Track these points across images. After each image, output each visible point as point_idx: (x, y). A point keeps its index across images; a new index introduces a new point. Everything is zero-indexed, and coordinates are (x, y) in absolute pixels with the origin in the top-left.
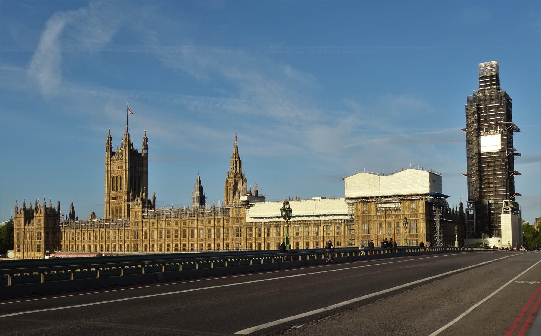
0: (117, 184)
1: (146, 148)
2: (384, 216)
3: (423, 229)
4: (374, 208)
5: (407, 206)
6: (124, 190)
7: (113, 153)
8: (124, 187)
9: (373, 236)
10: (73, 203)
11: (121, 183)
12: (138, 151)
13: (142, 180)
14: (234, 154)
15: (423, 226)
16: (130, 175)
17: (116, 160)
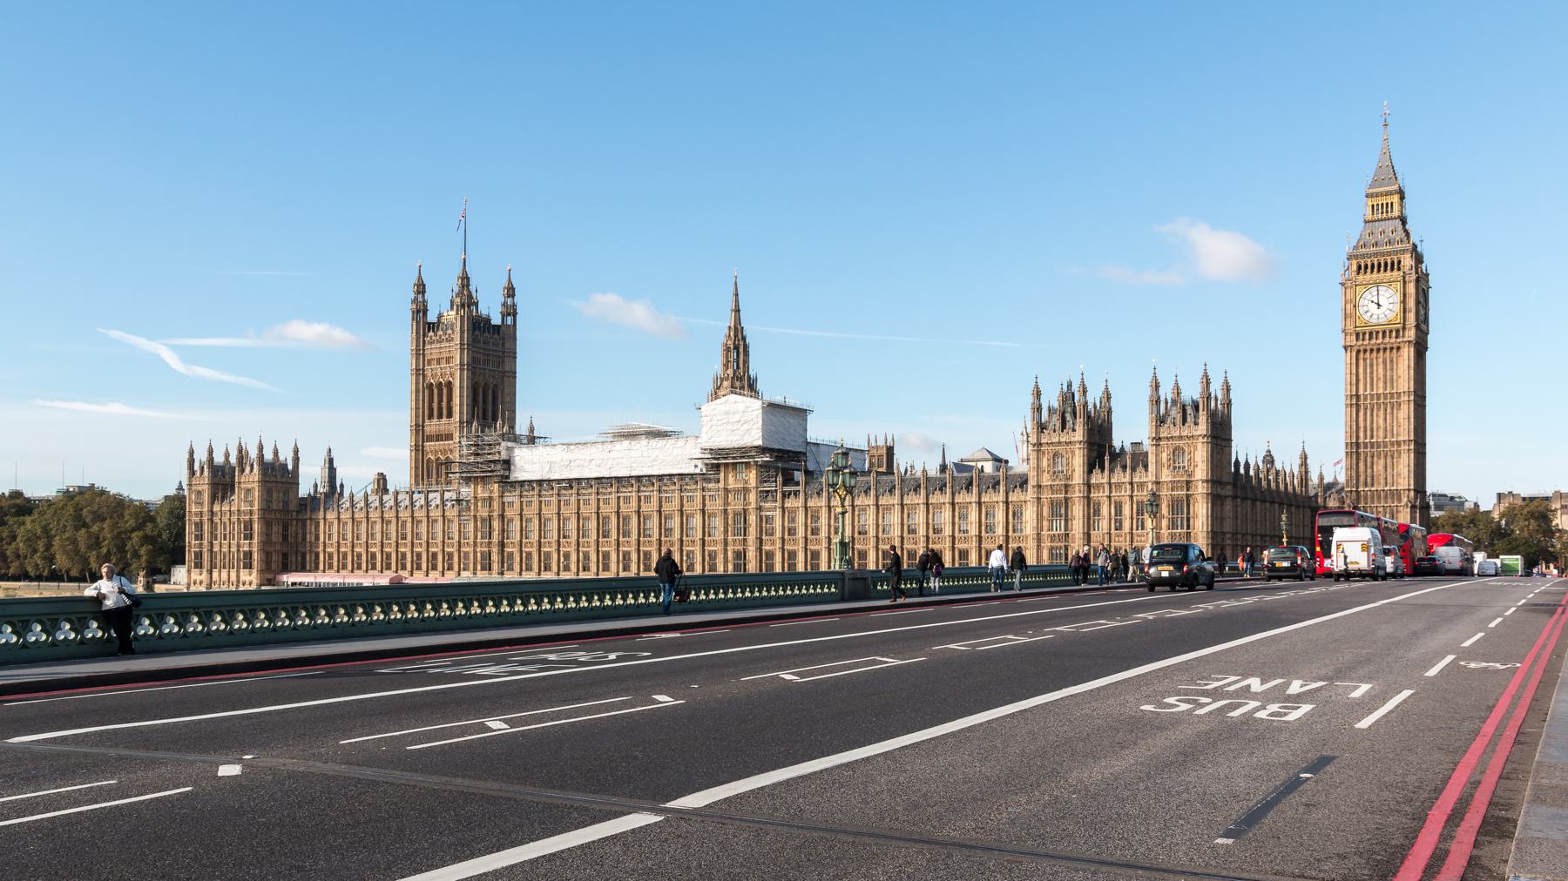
0: (440, 401)
1: (510, 311)
2: (1107, 487)
3: (1205, 518)
4: (1080, 466)
6: (457, 417)
7: (429, 324)
8: (456, 409)
9: (1077, 536)
10: (330, 450)
11: (450, 399)
12: (490, 320)
13: (503, 391)
15: (1205, 511)
16: (472, 380)
17: (438, 341)
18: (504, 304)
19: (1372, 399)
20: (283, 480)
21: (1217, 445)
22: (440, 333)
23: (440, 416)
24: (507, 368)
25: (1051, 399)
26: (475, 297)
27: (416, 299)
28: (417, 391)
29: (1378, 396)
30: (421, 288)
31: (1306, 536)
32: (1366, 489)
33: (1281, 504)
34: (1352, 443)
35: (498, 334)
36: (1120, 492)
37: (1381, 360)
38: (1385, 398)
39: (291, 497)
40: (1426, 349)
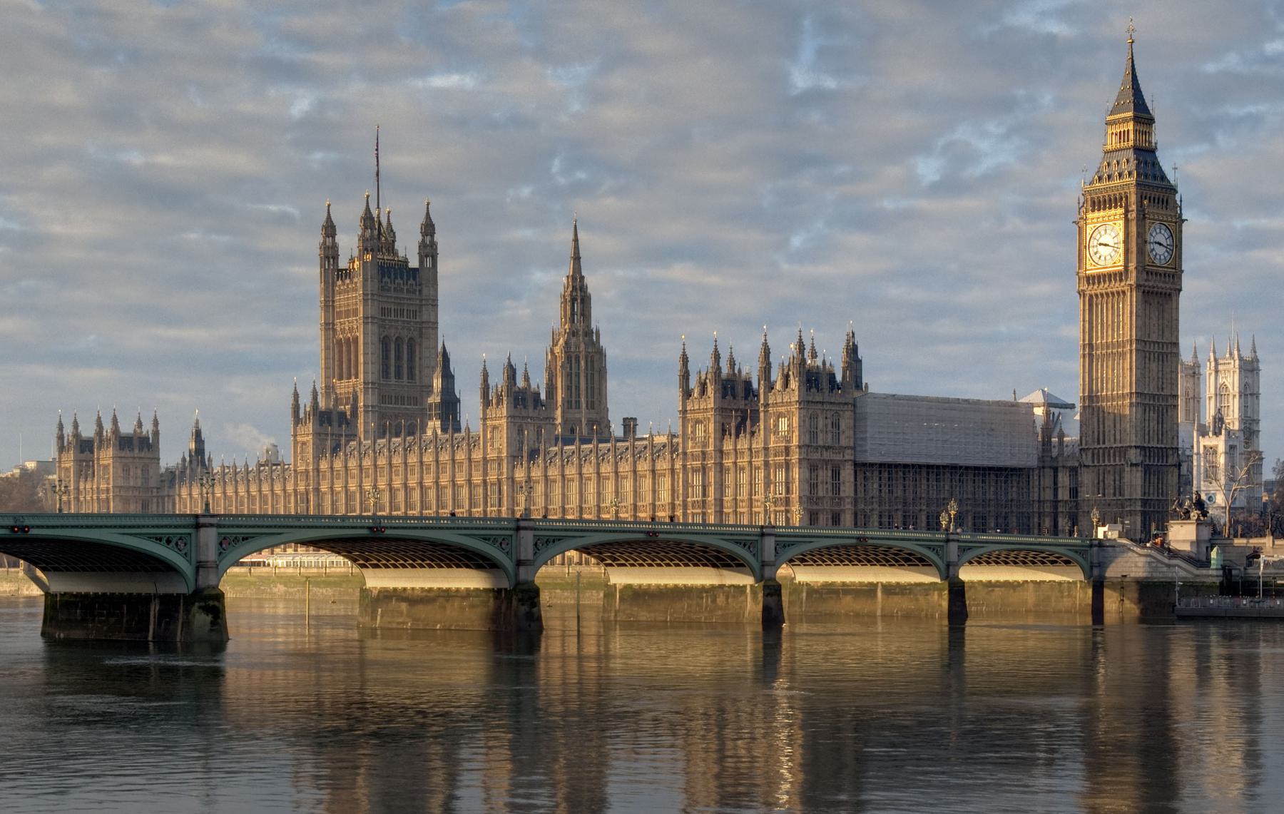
0: (349, 360)
1: (429, 250)
5: (772, 427)
6: (361, 376)
7: (342, 270)
12: (406, 262)
13: (420, 345)
14: (568, 277)
18: (423, 246)
19: (1102, 349)
20: (142, 455)
22: (348, 281)
23: (349, 377)
27: (324, 243)
28: (327, 348)
31: (1047, 498)
32: (1099, 446)
34: (1084, 397)
35: (414, 279)
37: (1110, 305)
39: (151, 472)
40: (1180, 290)
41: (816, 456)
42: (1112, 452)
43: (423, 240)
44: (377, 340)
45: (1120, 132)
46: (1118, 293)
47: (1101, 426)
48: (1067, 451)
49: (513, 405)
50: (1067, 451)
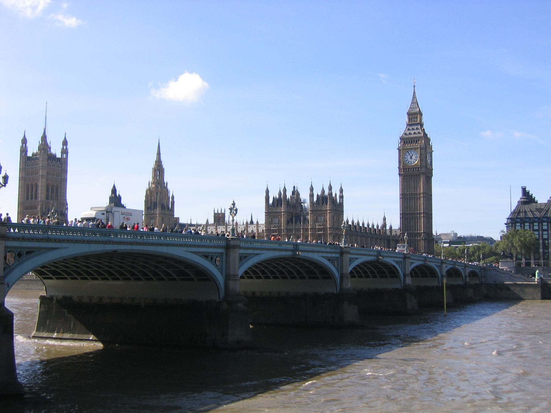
0: (32, 192)
1: (65, 151)
12: (55, 156)
19: (410, 196)
21: (336, 213)
23: (32, 198)
24: (63, 177)
25: (274, 194)
26: (49, 145)
27: (22, 146)
29: (412, 194)
30: (24, 141)
33: (381, 239)
35: (59, 161)
36: (299, 232)
37: (413, 180)
38: (415, 195)
40: (432, 176)
41: (334, 232)
42: (414, 234)
43: (63, 148)
44: (45, 184)
45: (415, 118)
46: (416, 175)
47: (409, 225)
48: (394, 233)
49: (161, 209)
50: (394, 233)
